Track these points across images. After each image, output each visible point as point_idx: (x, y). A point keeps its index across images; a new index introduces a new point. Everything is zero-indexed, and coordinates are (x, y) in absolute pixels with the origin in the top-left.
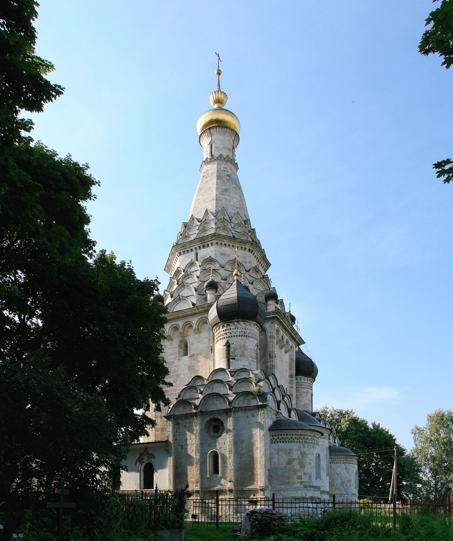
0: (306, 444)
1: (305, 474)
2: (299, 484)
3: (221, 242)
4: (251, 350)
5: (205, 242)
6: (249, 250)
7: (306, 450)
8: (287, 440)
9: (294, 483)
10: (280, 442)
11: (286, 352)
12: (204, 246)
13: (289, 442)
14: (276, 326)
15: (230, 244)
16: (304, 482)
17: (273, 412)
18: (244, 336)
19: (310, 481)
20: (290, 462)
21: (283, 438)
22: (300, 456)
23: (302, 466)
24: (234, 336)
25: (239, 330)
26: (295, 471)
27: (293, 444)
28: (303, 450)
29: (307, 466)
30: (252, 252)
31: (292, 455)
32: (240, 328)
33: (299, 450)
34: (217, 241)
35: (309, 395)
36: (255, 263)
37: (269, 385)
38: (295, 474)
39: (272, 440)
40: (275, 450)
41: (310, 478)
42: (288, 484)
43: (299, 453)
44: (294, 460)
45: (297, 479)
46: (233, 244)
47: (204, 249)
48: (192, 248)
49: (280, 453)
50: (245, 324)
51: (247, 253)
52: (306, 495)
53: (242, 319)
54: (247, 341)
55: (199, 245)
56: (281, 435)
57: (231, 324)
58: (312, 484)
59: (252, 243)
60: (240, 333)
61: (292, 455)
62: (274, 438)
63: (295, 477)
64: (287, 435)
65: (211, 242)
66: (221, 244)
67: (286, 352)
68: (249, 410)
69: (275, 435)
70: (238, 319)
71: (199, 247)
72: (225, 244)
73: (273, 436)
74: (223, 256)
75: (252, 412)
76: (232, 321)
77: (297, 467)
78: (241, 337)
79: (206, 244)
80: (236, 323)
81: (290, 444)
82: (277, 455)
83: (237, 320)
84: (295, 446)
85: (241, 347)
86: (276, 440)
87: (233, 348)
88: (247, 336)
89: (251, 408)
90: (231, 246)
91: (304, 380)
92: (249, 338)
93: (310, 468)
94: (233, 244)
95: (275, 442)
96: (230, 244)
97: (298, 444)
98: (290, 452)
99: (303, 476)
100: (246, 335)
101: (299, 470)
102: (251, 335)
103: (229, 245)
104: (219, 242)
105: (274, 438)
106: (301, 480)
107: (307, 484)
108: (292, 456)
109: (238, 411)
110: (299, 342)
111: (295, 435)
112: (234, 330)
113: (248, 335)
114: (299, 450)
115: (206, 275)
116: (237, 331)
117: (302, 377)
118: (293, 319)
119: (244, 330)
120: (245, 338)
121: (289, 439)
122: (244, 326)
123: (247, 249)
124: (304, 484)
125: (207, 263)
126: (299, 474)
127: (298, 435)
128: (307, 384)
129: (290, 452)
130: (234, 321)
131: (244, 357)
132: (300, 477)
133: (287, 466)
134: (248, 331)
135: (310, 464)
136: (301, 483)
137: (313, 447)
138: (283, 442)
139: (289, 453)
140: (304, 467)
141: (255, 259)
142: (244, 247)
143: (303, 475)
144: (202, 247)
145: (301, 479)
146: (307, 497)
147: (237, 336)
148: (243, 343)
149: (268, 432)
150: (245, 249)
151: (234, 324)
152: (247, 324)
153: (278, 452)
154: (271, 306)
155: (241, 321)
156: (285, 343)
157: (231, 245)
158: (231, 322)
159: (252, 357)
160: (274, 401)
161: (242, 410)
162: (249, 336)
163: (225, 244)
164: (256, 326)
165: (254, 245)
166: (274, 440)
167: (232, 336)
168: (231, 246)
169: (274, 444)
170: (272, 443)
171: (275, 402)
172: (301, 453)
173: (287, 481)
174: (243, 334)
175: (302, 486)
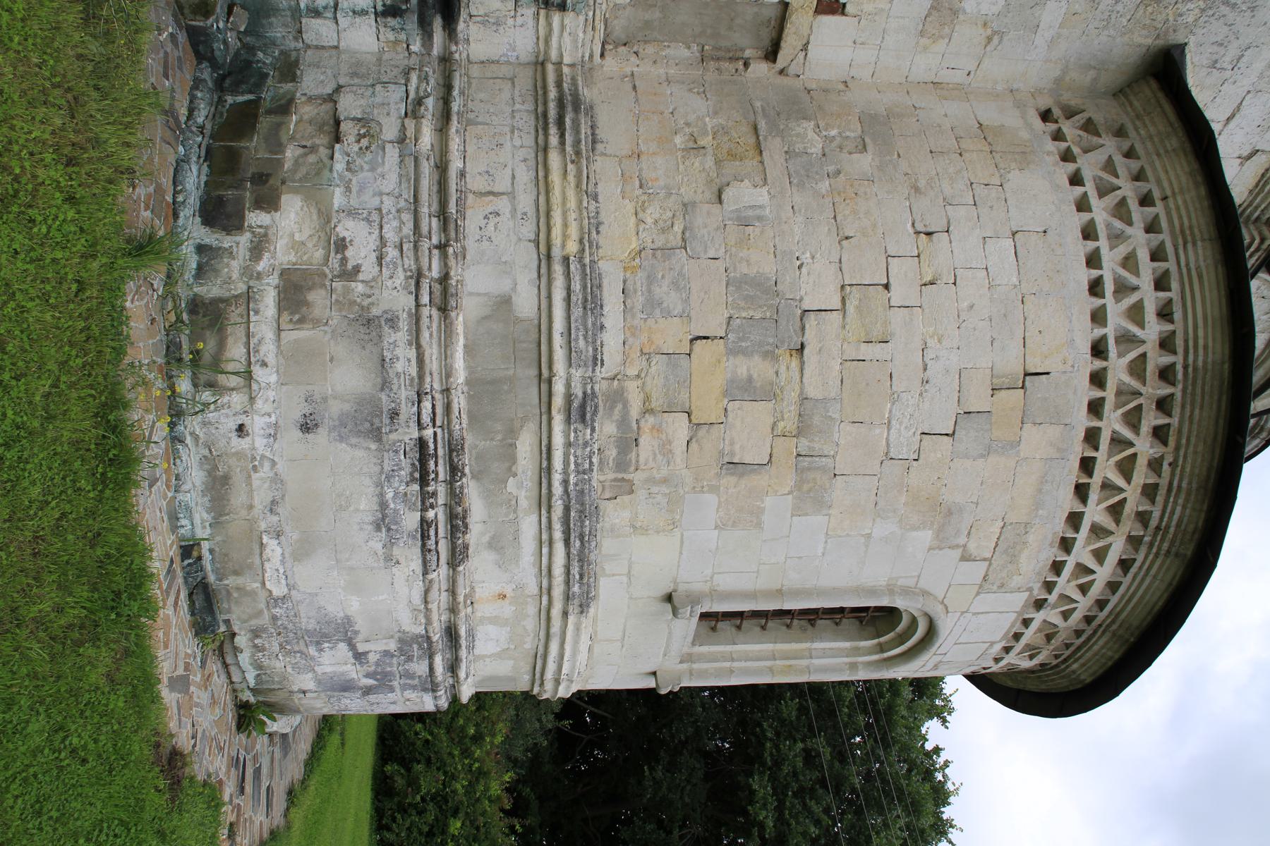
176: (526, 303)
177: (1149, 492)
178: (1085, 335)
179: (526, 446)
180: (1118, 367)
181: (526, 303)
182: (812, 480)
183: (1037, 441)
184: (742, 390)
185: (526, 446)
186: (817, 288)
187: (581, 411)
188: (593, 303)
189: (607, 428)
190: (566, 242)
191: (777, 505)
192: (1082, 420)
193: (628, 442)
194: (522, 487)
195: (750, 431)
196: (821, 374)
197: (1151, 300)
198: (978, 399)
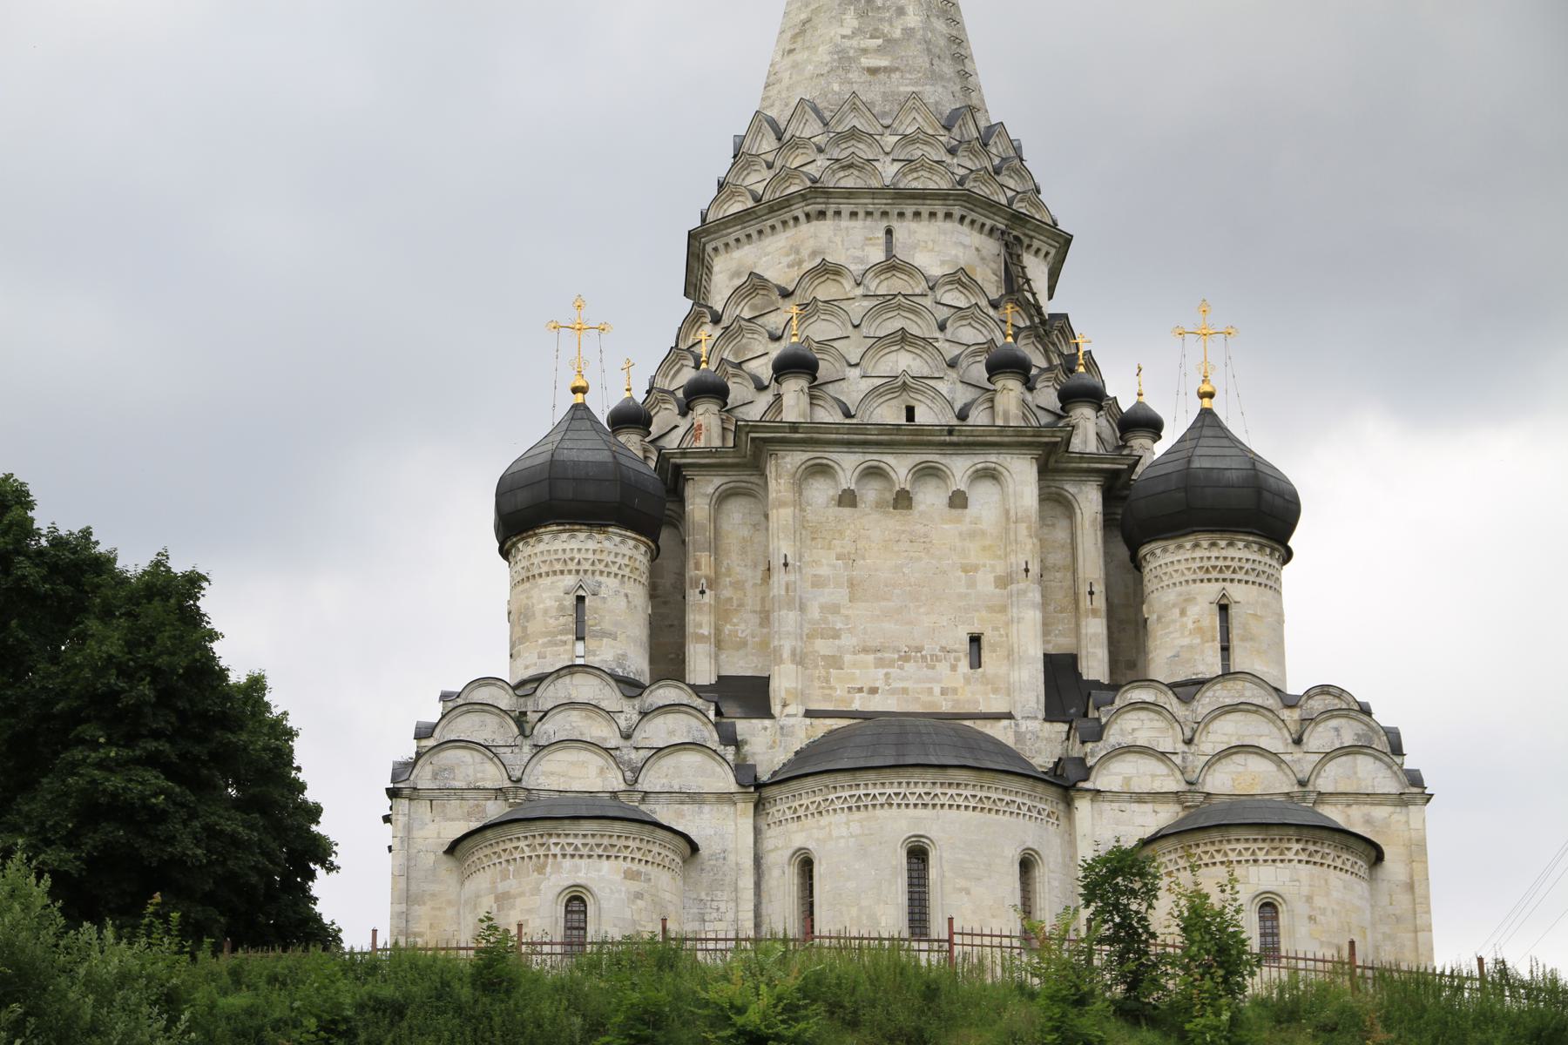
3: (725, 240)
4: (546, 611)
6: (808, 216)
7: (511, 885)
28: (502, 887)
30: (822, 214)
34: (714, 244)
54: (535, 593)
66: (727, 245)
72: (738, 240)
90: (755, 235)
92: (540, 581)
94: (758, 227)
104: (720, 244)
113: (536, 572)
123: (802, 218)
137: (540, 869)
142: (787, 217)
149: (444, 858)
150: (796, 219)
152: (532, 541)
157: (753, 231)
163: (738, 240)
164: (565, 536)
177: (1213, 843)
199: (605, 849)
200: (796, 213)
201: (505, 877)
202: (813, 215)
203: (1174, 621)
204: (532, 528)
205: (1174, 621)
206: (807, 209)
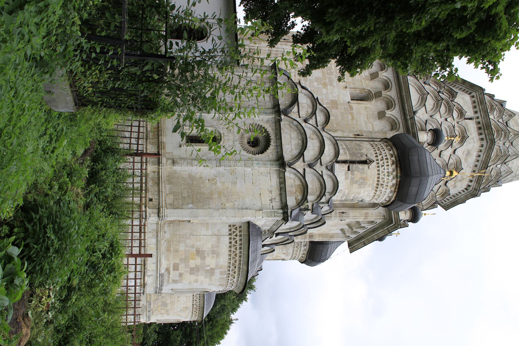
0: (225, 276)
1: (181, 275)
2: (166, 267)
3: (483, 151)
4: (359, 193)
5: (484, 130)
6: (469, 186)
8: (233, 249)
9: (168, 259)
10: (230, 238)
11: (342, 230)
12: (480, 128)
13: (230, 251)
14: (378, 221)
15: (480, 162)
16: (169, 273)
17: (275, 227)
18: (378, 184)
19: (171, 281)
20: (199, 253)
21: (236, 242)
22: (209, 268)
23: (193, 271)
24: (379, 170)
25: (386, 177)
26: (186, 260)
27: (227, 257)
28: (217, 272)
29: (193, 277)
30: (466, 189)
31: (211, 255)
32: (388, 179)
33: (218, 266)
34: (485, 146)
35: (283, 257)
36: (453, 192)
37: (312, 220)
38: (181, 260)
39: (233, 226)
40: (219, 231)
41: (175, 281)
42: (167, 250)
43: (213, 266)
44: (203, 258)
45: (174, 264)
46: (478, 167)
47: (476, 129)
48: (479, 113)
49: (214, 239)
50: (393, 185)
51: (465, 183)
52: (149, 276)
53: (400, 181)
54: (370, 189)
55: (481, 122)
56: (241, 240)
57: (394, 166)
58: (165, 284)
59: (477, 190)
60: (383, 178)
61: (211, 255)
62: (236, 229)
63: (177, 261)
64: (240, 248)
65: (485, 138)
66: (481, 151)
67: (342, 230)
68: (281, 194)
69: (240, 231)
70: (401, 177)
71: (479, 123)
73: (240, 227)
74: (466, 152)
75: (278, 199)
76: (399, 168)
77: (192, 263)
78: (376, 179)
79: (482, 131)
80: (395, 173)
81: (227, 253)
82: (211, 234)
83: (399, 175)
84: (224, 260)
85: (364, 180)
86: (234, 232)
87: (363, 169)
88: (377, 188)
89: (283, 198)
90: (477, 163)
91: (303, 251)
92: (374, 191)
93: (190, 282)
94: (478, 167)
95: (230, 230)
96: (480, 162)
97: (227, 264)
98: (214, 254)
99: (177, 272)
100: (379, 186)
101: (187, 266)
102: (378, 193)
103: (478, 161)
104: (483, 149)
105: (236, 229)
106: (171, 270)
107: (166, 277)
108: (208, 256)
109: (280, 178)
110: (353, 246)
111: (240, 260)
112: (386, 171)
113: (378, 190)
114: (218, 266)
115: (448, 130)
116: (384, 175)
117: (307, 248)
118: (381, 239)
119: (385, 184)
120: (375, 185)
121: (234, 252)
122: (390, 184)
123: (470, 184)
124: (166, 274)
125: (460, 132)
126: (182, 267)
127: (240, 264)
128: (298, 254)
129: (215, 253)
130: (399, 171)
131: (350, 184)
132: (176, 267)
133: (195, 249)
134: (383, 190)
135: (196, 281)
136: (168, 270)
138: (230, 243)
139: (213, 252)
140: (191, 274)
141: (457, 192)
143: (180, 271)
144: (479, 126)
145: (174, 270)
146: (146, 278)
147: (378, 174)
148: (369, 183)
150: (471, 181)
151: (393, 171)
153: (215, 235)
154: (404, 215)
155: (397, 181)
156: (355, 230)
158: (396, 166)
159: (348, 194)
160: (290, 229)
161: (280, 183)
162: (376, 191)
164: (388, 199)
165: (474, 191)
166: (233, 230)
167: (378, 167)
168: (477, 163)
169: (228, 228)
170: (230, 226)
171: (287, 229)
172: (212, 269)
173: (172, 249)
174: (381, 182)
175: (163, 271)
176: (145, 304)
178: (191, 304)
179: (145, 313)
180: (195, 306)
181: (145, 304)
182: (168, 314)
183: (187, 311)
184: (163, 309)
185: (145, 313)
186: (168, 302)
187: (149, 311)
188: (150, 304)
189: (151, 312)
190: (148, 300)
191: (165, 316)
192: (191, 310)
193: (153, 312)
194: (145, 315)
195: (163, 311)
196: (169, 308)
197: (198, 301)
198: (182, 309)
199: (234, 245)
200: (473, 182)
201: (221, 273)
202: (468, 188)
203: (282, 251)
204: (398, 192)
205: (282, 251)
206: (471, 188)
